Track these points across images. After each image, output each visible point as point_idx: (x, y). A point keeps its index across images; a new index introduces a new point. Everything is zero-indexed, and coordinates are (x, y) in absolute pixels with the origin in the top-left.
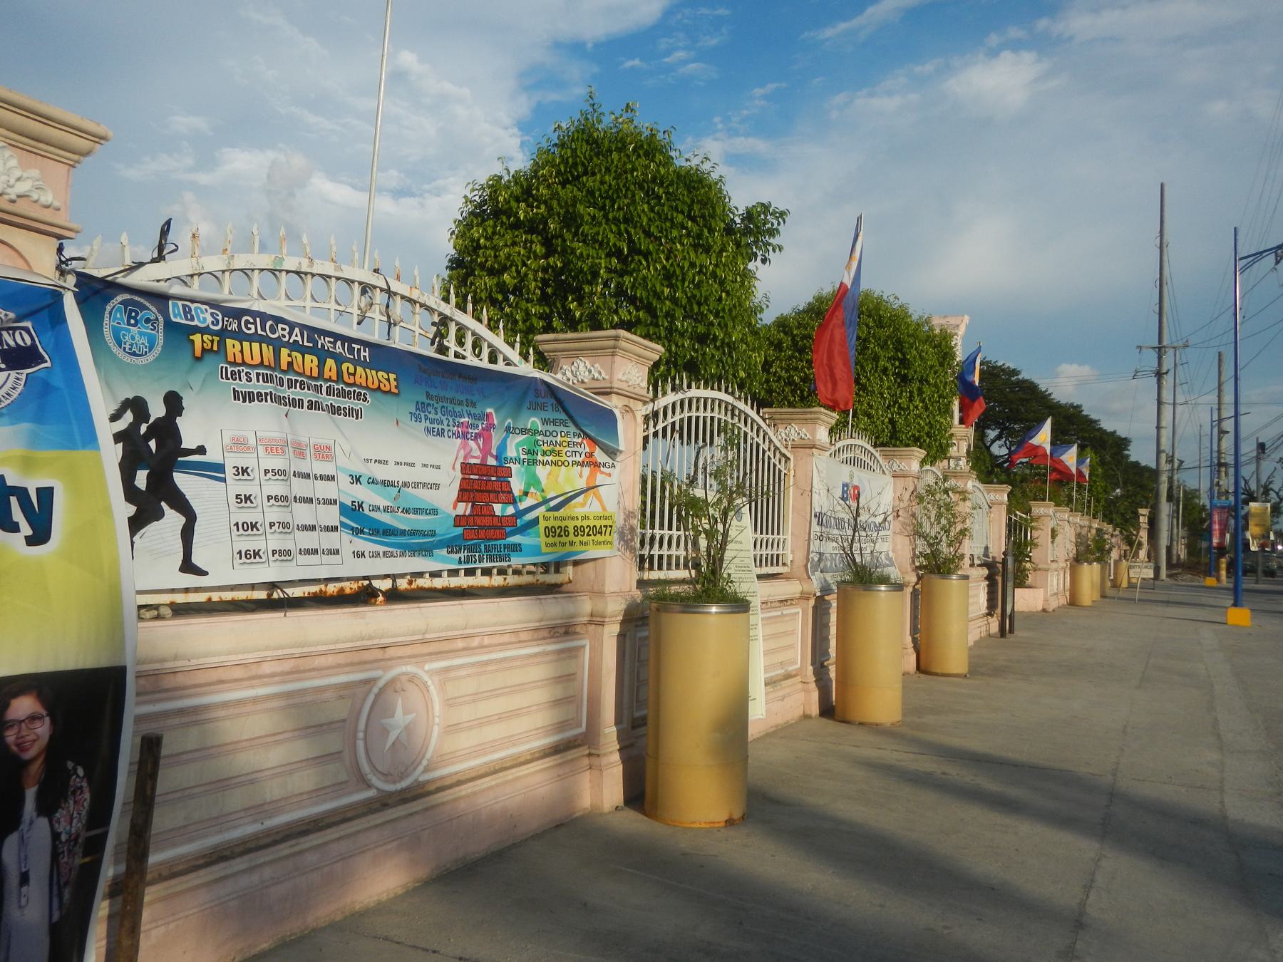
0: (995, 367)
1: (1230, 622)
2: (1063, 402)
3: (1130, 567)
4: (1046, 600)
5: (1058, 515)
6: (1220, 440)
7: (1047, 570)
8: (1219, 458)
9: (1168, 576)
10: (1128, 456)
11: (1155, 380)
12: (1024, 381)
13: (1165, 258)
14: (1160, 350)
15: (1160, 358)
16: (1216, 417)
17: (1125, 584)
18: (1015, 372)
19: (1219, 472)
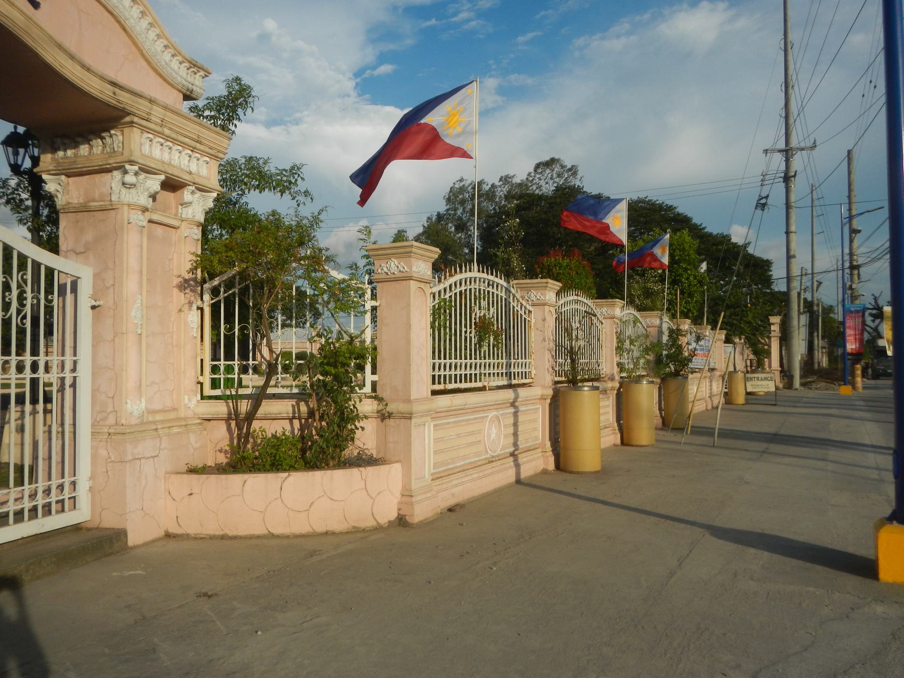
0: (653, 204)
1: (887, 573)
2: (715, 233)
3: (746, 379)
4: (407, 494)
5: (534, 295)
6: (851, 241)
7: (409, 417)
8: (851, 261)
9: (802, 384)
10: (772, 275)
11: (783, 185)
12: (679, 214)
13: (790, 58)
14: (788, 153)
15: (787, 161)
16: (845, 214)
17: (740, 399)
18: (670, 208)
19: (852, 275)
